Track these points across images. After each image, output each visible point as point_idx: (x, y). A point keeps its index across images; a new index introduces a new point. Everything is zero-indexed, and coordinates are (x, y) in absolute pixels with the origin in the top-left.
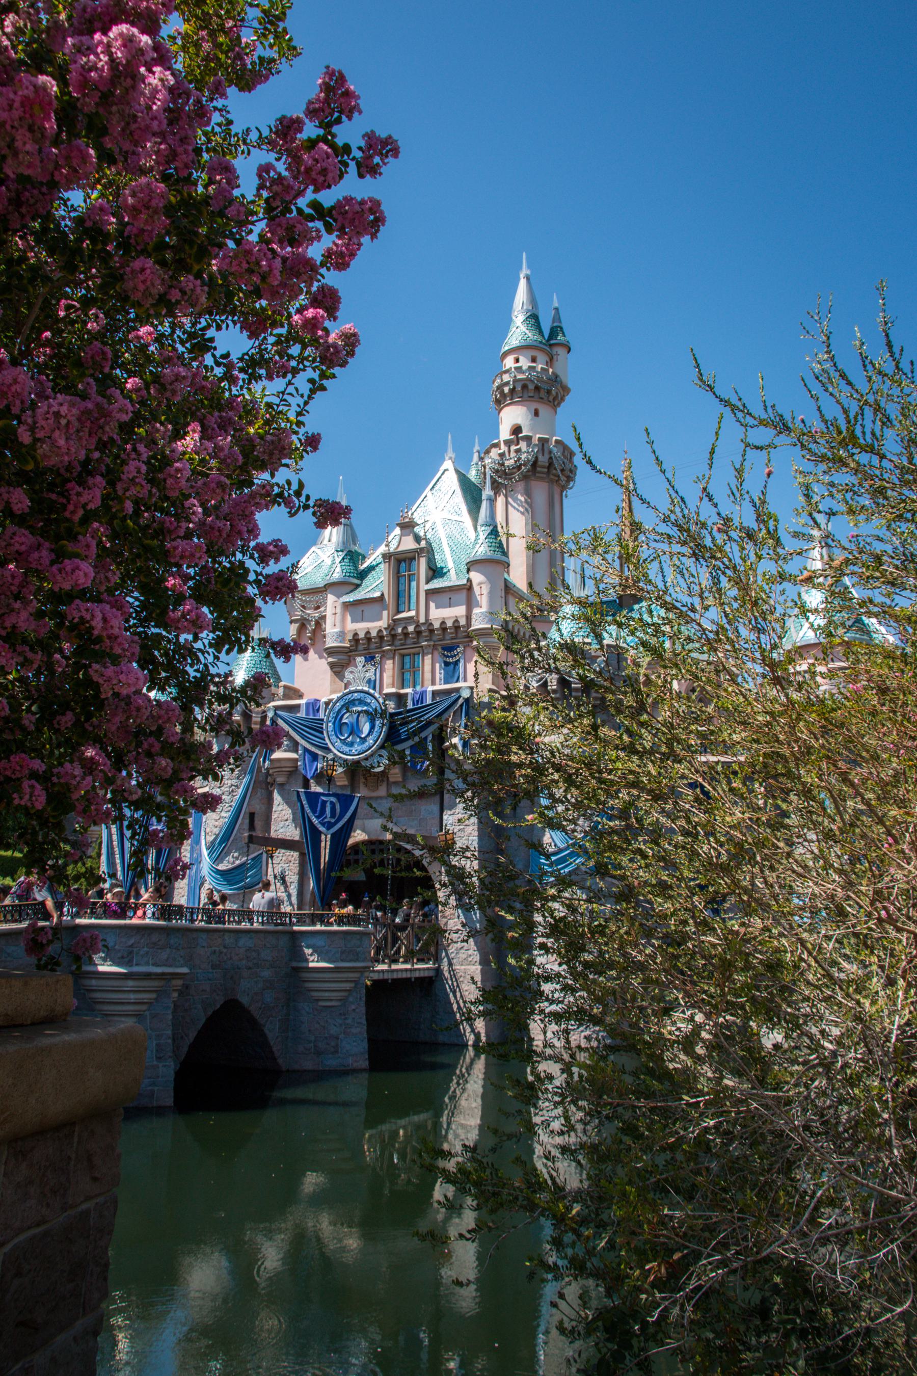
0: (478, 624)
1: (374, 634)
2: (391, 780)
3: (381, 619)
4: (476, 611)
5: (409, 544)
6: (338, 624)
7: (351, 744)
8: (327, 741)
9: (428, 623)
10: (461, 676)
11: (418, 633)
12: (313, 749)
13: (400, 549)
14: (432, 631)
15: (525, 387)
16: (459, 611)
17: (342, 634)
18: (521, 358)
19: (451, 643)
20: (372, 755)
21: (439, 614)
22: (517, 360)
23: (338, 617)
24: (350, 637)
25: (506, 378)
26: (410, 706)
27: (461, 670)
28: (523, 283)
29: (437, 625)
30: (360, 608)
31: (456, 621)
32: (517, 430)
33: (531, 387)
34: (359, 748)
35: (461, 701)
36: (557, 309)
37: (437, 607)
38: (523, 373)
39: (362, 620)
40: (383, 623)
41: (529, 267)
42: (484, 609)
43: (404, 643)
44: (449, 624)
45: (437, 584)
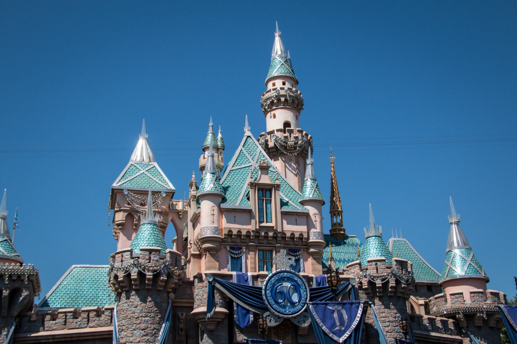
0: (313, 239)
1: (244, 233)
2: (300, 333)
3: (250, 224)
4: (313, 230)
5: (265, 180)
6: (216, 222)
7: (284, 307)
8: (266, 302)
9: (283, 233)
10: (302, 269)
11: (275, 237)
12: (247, 307)
13: (260, 182)
14: (284, 237)
15: (293, 101)
16: (303, 228)
17: (218, 230)
18: (287, 83)
19: (297, 247)
20: (299, 315)
21: (289, 228)
22: (284, 84)
23: (216, 217)
24: (225, 232)
25: (282, 92)
26: (314, 286)
27: (302, 265)
28: (277, 40)
29: (288, 235)
30: (233, 214)
31: (301, 234)
32: (287, 124)
33: (296, 102)
34: (292, 310)
35: (350, 286)
36: (290, 59)
37: (288, 224)
38: (292, 92)
39: (235, 223)
40: (252, 227)
41: (280, 30)
42: (318, 230)
43: (266, 243)
44: (297, 235)
45: (285, 209)
